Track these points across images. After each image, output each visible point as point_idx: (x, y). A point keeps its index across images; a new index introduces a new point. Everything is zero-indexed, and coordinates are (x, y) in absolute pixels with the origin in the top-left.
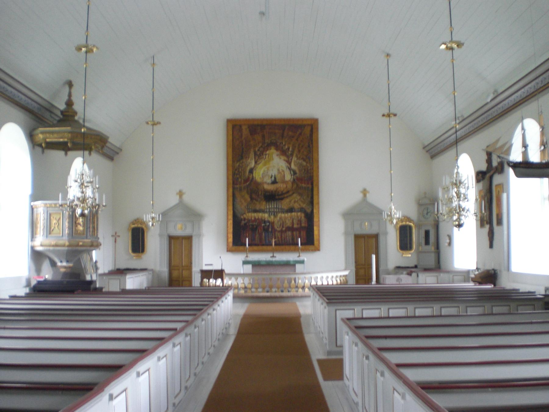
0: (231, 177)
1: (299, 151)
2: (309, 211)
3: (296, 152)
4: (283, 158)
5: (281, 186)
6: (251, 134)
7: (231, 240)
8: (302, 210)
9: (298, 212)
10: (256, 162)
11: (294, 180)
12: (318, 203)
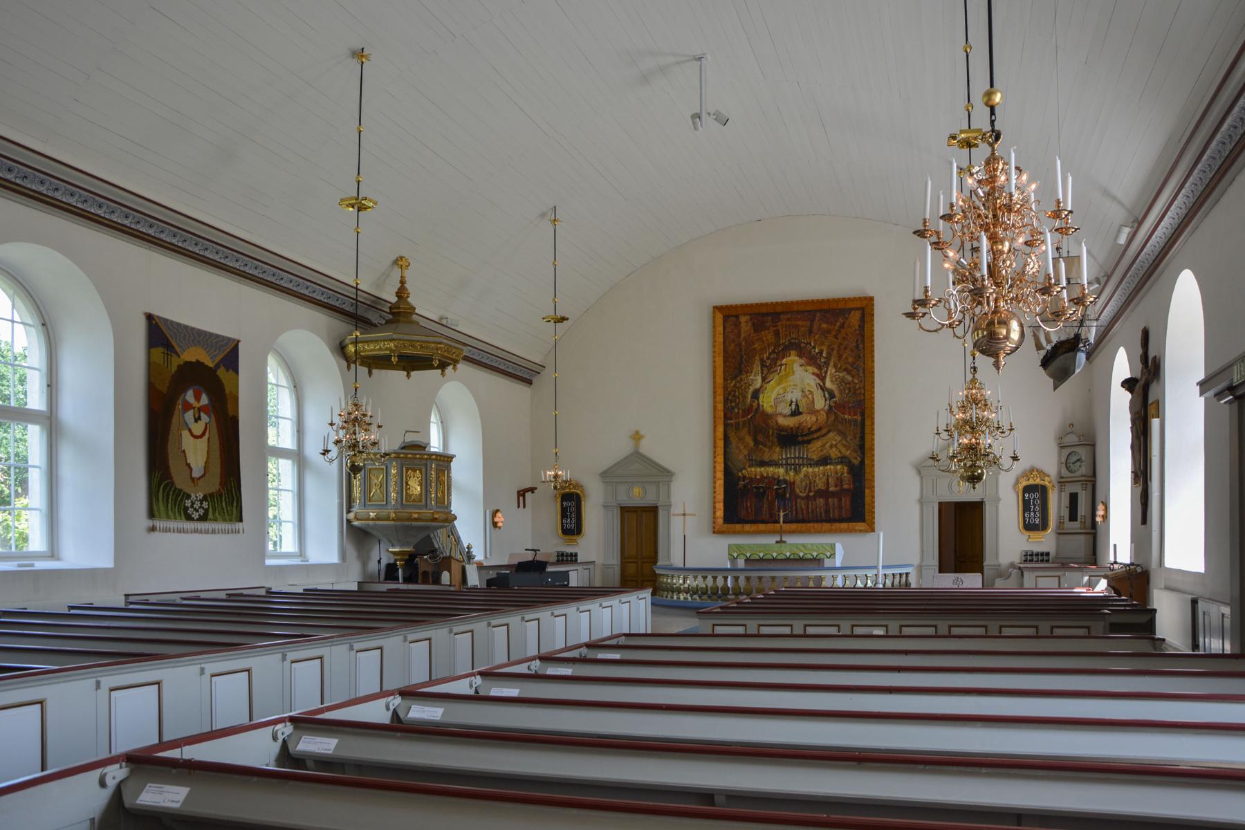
0: (720, 406)
1: (840, 356)
2: (856, 462)
3: (833, 360)
4: (811, 369)
5: (808, 420)
6: (756, 331)
7: (720, 513)
8: (843, 460)
9: (837, 464)
10: (764, 379)
11: (830, 407)
12: (872, 449)
